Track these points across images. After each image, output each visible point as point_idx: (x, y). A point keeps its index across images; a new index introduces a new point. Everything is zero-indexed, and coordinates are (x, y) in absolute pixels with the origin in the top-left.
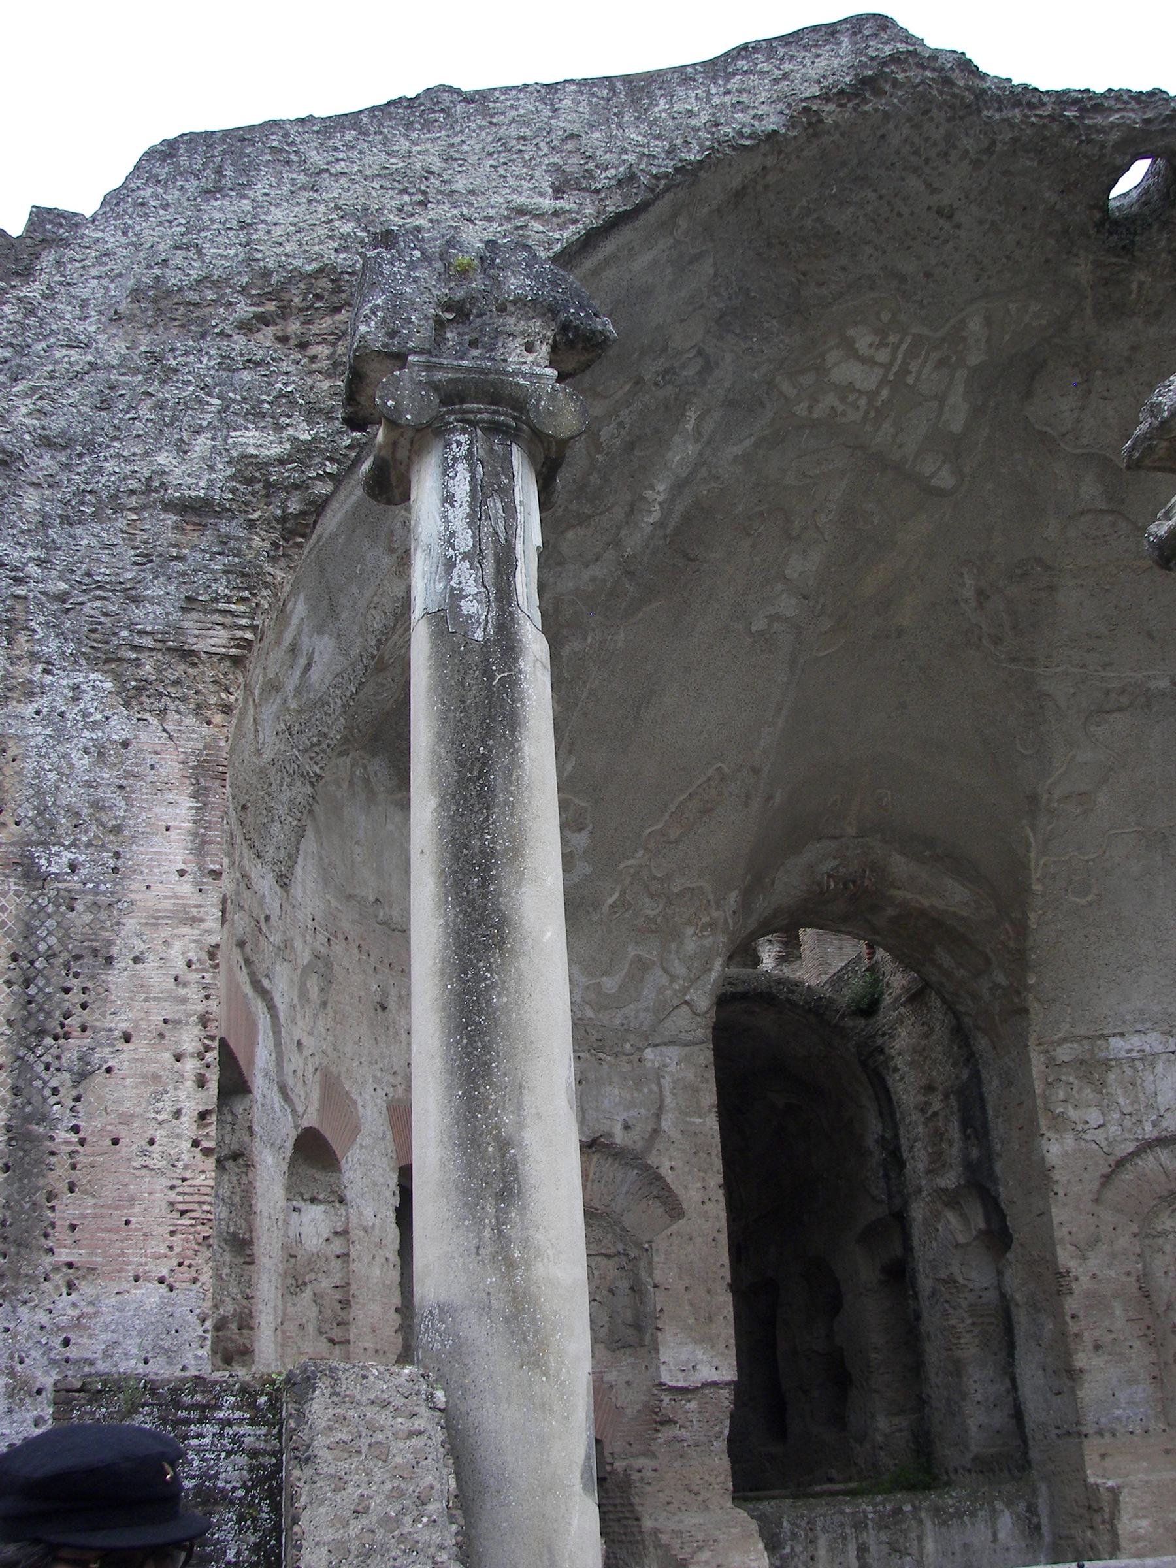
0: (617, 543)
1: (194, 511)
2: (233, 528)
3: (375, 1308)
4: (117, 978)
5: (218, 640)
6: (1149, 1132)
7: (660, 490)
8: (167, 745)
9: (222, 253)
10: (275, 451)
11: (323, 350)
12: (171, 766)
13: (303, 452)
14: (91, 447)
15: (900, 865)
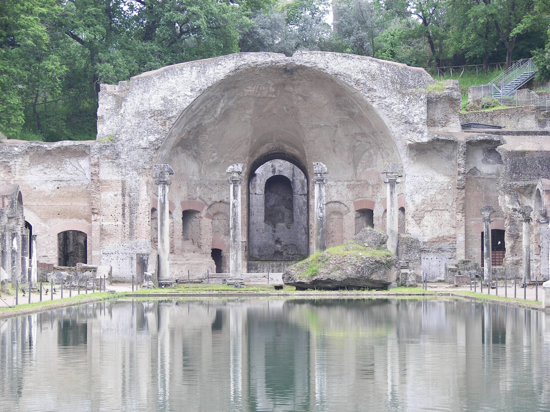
0: (213, 116)
1: (145, 149)
2: (149, 151)
3: (178, 232)
4: (139, 207)
5: (148, 167)
6: (329, 200)
7: (219, 110)
8: (143, 180)
9: (146, 106)
10: (154, 140)
11: (159, 121)
12: (144, 183)
13: (157, 140)
14: (132, 140)
15: (286, 146)
